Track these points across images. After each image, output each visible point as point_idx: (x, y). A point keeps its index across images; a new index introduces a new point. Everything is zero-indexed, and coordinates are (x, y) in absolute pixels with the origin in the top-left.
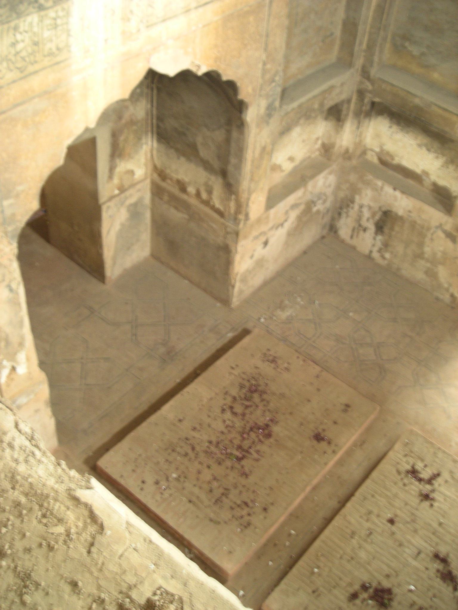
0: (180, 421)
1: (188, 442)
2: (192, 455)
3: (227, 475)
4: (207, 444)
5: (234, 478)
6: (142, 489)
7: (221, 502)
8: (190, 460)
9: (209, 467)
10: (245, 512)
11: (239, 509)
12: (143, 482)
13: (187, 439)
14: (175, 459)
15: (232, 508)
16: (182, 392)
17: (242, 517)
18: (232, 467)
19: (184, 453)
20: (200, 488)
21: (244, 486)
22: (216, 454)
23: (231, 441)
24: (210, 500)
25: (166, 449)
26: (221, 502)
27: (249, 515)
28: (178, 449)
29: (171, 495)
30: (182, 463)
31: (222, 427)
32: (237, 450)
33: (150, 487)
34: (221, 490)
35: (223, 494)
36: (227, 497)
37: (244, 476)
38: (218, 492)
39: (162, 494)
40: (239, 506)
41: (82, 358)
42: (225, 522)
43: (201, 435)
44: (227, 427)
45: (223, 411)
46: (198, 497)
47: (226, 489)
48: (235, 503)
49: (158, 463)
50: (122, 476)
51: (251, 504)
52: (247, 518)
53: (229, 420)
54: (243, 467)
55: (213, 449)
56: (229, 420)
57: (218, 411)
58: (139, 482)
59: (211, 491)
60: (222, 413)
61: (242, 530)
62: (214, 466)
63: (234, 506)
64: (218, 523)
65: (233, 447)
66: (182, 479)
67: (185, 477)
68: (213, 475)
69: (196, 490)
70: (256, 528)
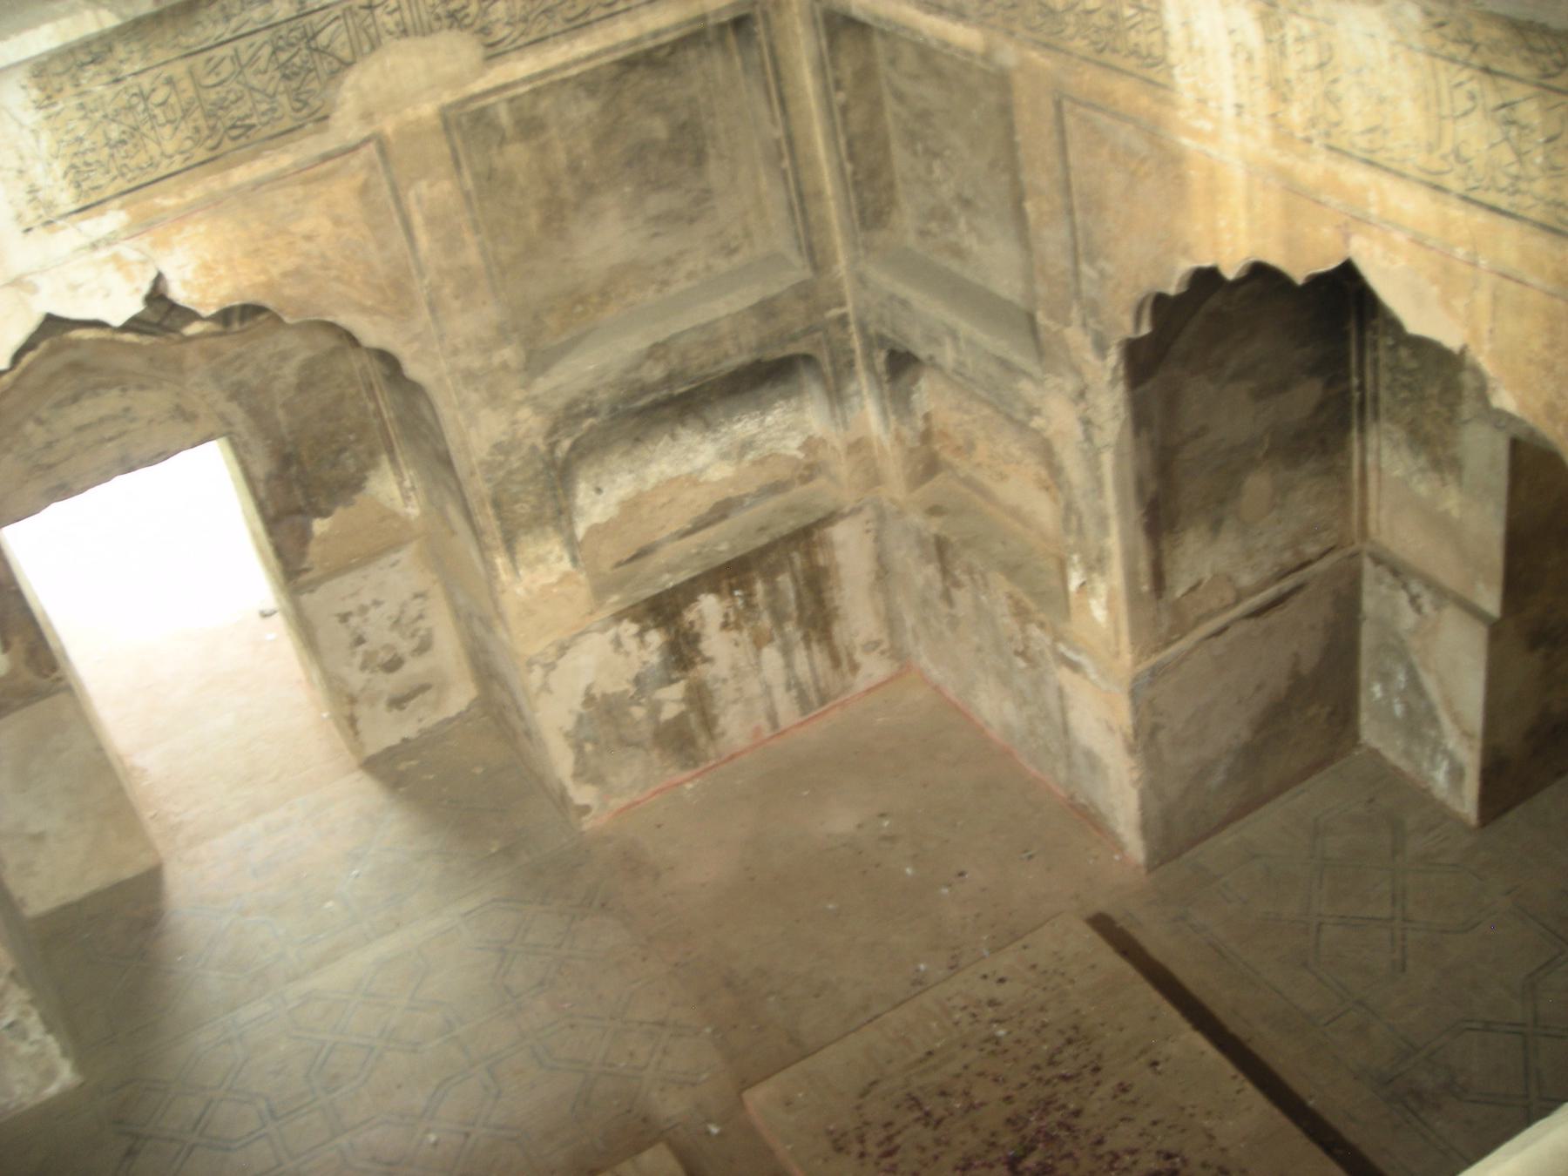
0: (1155, 1064)
1: (1086, 1072)
2: (1048, 1073)
3: (975, 1130)
4: (1072, 1106)
5: (963, 1143)
6: (985, 977)
7: (910, 1108)
8: (1037, 1067)
9: (1008, 1099)
10: (873, 1150)
11: (882, 1134)
12: (1002, 981)
13: (1097, 1070)
14: (1044, 1041)
15: (888, 1125)
16: (1241, 1077)
17: (862, 1140)
18: (993, 1144)
19: (1057, 1058)
20: (958, 1076)
21: (936, 1158)
22: (1041, 1119)
23: (1070, 1155)
24: (921, 1088)
25: (1076, 1028)
26: (910, 1108)
27: (862, 1155)
28: (1071, 1050)
29: (956, 1024)
30: (1030, 1052)
31: (1114, 1143)
32: (1039, 1164)
33: (983, 991)
34: (939, 1112)
35: (928, 1114)
36: (918, 1120)
37: (961, 1163)
38: (935, 1105)
39: (965, 1008)
40: (889, 1138)
41: (1404, 920)
42: (858, 1107)
43: (1100, 1099)
44: (1116, 1157)
45: (1169, 1156)
46: (935, 1068)
47: (939, 1122)
48: (899, 1132)
49: (1042, 1009)
50: (1025, 947)
51: (886, 1162)
52: (856, 1148)
53: (1135, 1163)
54: (991, 1166)
55: (1056, 1116)
56: (1135, 1163)
57: (1169, 1145)
58: (1001, 974)
59: (943, 1094)
60: (1159, 1152)
61: (831, 1133)
62: (1008, 1111)
63: (892, 1130)
64: (863, 1095)
65: (1051, 1157)
66: (989, 1047)
67: (993, 1053)
68: (982, 1104)
69: (954, 1067)
70: (826, 1160)
